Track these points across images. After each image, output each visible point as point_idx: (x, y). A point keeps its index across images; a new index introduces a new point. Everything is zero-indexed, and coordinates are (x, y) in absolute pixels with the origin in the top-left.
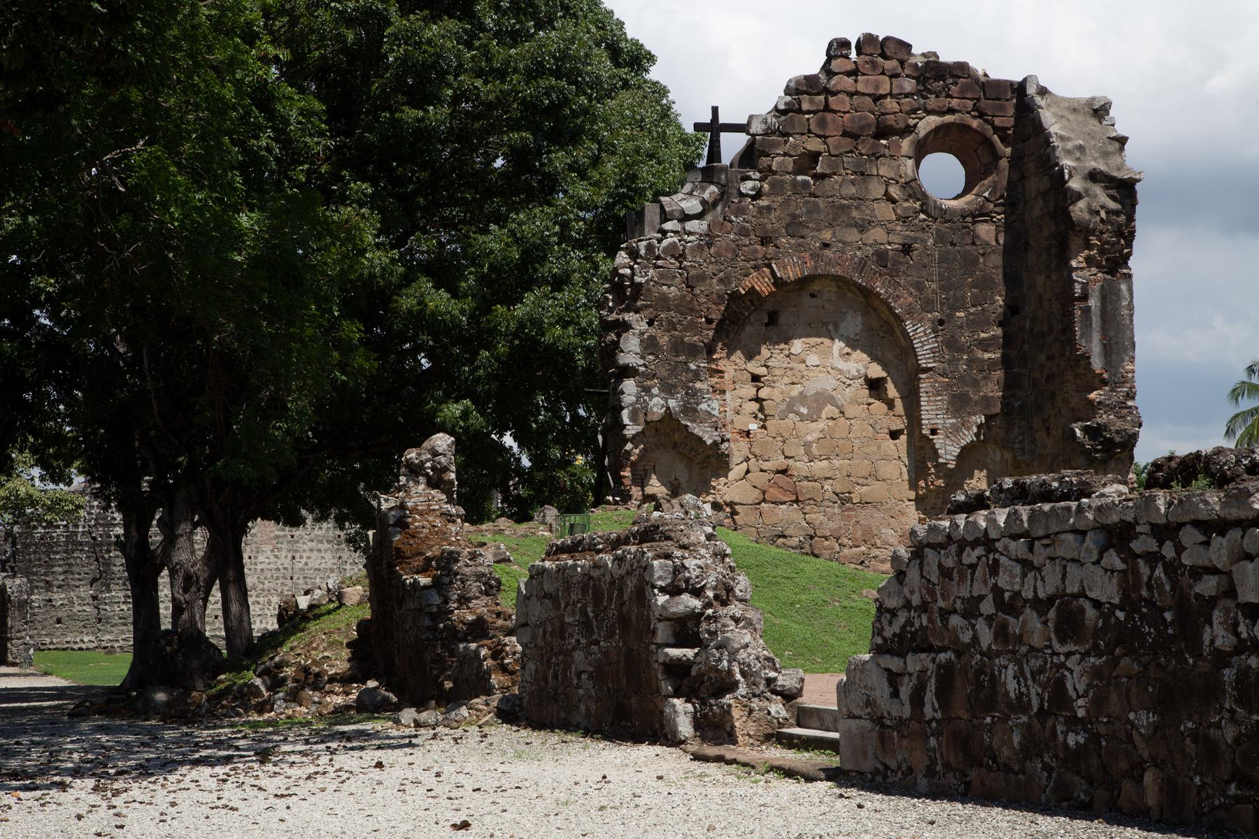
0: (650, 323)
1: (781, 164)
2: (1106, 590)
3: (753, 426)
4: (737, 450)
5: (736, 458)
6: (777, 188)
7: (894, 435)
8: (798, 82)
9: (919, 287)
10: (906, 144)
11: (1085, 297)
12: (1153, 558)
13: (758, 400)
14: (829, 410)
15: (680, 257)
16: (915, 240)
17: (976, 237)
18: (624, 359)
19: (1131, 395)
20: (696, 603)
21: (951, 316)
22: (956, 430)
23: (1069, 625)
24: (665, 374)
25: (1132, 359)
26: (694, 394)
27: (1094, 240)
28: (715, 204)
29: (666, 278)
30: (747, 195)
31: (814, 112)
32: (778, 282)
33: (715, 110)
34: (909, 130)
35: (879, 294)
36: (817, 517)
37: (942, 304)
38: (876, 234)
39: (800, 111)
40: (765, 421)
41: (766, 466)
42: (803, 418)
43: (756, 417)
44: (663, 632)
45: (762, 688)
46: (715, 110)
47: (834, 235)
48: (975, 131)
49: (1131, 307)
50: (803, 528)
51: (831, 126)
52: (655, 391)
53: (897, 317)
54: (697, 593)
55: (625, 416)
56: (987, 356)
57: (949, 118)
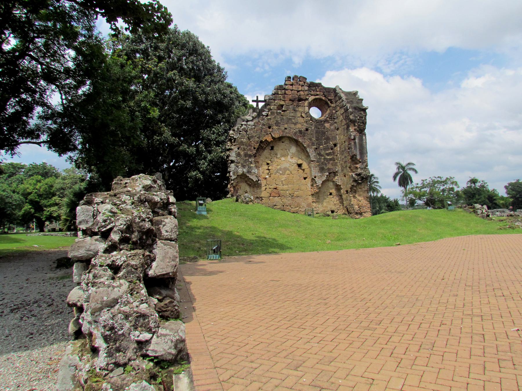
0: (238, 149)
1: (273, 107)
3: (267, 177)
4: (263, 182)
5: (263, 185)
6: (272, 113)
7: (305, 178)
8: (277, 87)
9: (310, 139)
10: (306, 103)
11: (354, 139)
13: (268, 169)
14: (288, 172)
15: (246, 131)
16: (309, 127)
17: (325, 127)
19: (367, 166)
21: (319, 147)
22: (321, 176)
24: (242, 162)
25: (367, 156)
26: (250, 167)
27: (356, 124)
28: (256, 117)
29: (243, 137)
30: (264, 115)
31: (282, 94)
32: (273, 138)
33: (257, 97)
34: (307, 99)
35: (300, 141)
36: (285, 200)
37: (317, 144)
38: (299, 126)
39: (278, 94)
40: (270, 175)
41: (271, 187)
42: (281, 174)
43: (268, 174)
45: (130, 354)
46: (257, 97)
47: (288, 126)
48: (323, 100)
49: (366, 143)
50: (281, 203)
51: (286, 98)
52: (240, 167)
53: (305, 147)
56: (328, 157)
57: (317, 97)
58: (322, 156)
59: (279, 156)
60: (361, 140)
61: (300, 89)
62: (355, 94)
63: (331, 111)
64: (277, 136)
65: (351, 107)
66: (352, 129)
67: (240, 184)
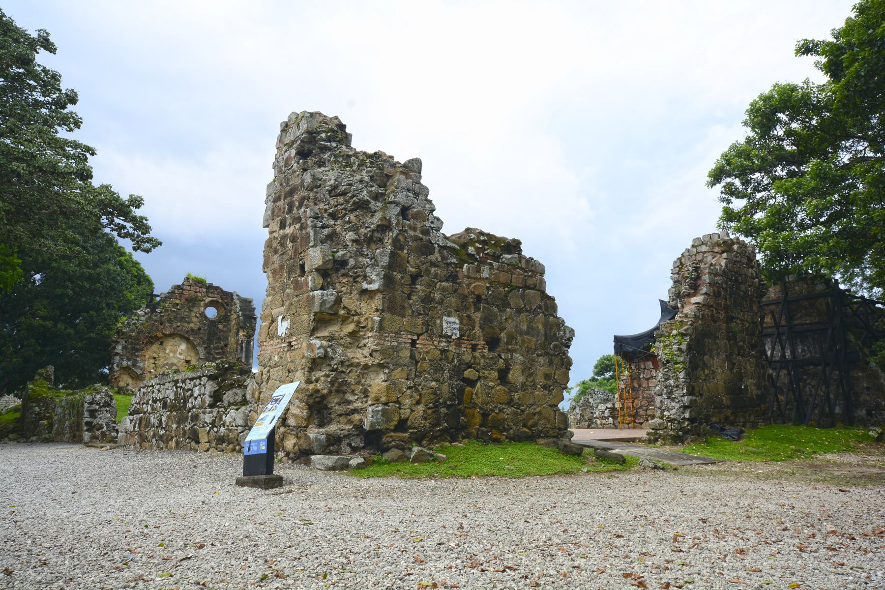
0: (126, 342)
2: (172, 396)
3: (152, 371)
11: (242, 343)
12: (181, 387)
13: (154, 364)
18: (116, 351)
20: (97, 407)
23: (165, 406)
26: (135, 362)
29: (132, 331)
34: (203, 300)
38: (192, 325)
44: (86, 414)
54: (98, 404)
55: (115, 366)
58: (211, 354)
59: (167, 351)
60: (248, 343)
61: (198, 290)
62: (250, 302)
63: (226, 313)
64: (168, 333)
65: (243, 315)
66: (241, 333)
67: (122, 376)
